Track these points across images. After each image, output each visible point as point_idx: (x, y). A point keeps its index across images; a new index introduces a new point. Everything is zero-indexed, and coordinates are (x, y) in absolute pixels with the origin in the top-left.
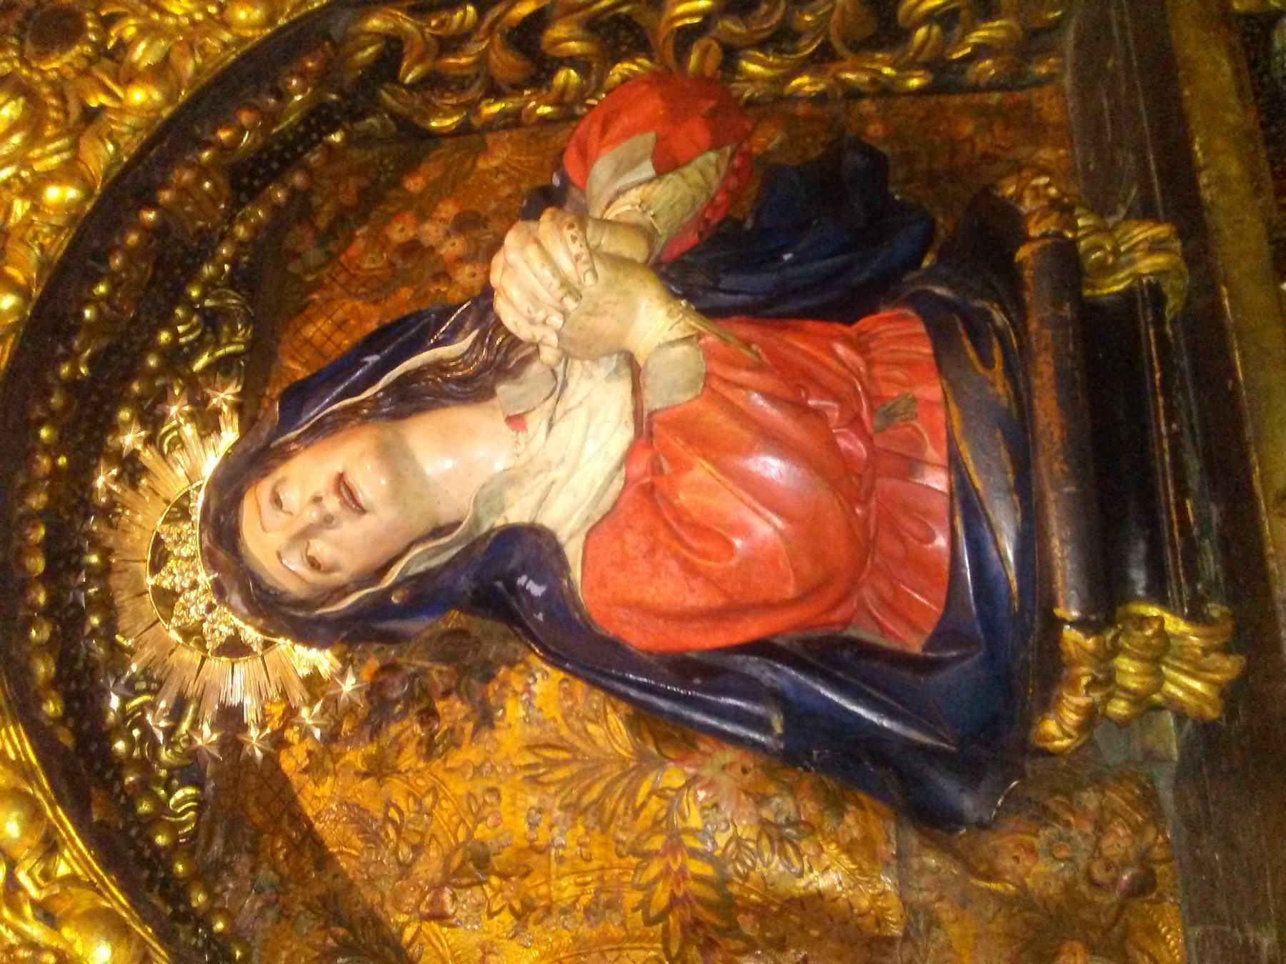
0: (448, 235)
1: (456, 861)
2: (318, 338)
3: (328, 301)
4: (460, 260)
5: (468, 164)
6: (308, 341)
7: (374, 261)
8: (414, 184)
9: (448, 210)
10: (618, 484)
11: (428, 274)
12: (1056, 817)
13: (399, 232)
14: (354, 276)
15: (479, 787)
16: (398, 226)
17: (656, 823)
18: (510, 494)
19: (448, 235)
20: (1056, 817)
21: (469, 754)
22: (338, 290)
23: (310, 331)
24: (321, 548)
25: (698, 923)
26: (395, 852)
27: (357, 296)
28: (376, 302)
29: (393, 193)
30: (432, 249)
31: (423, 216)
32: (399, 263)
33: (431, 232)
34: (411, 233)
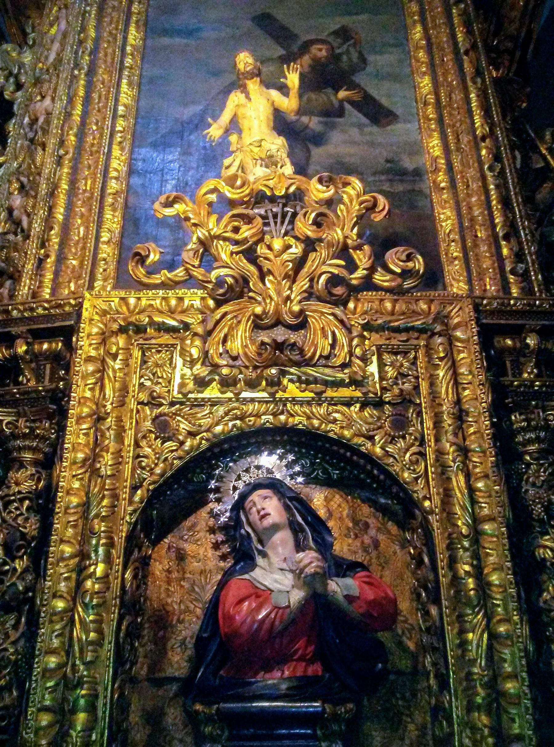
0: (371, 538)
1: (182, 552)
2: (335, 500)
3: (347, 502)
4: (363, 542)
5: (397, 543)
6: (334, 496)
7: (362, 514)
8: (391, 525)
9: (381, 537)
10: (263, 588)
11: (357, 532)
12: (184, 728)
13: (372, 521)
14: (356, 509)
15: (201, 556)
16: (374, 521)
17: (188, 607)
18: (266, 560)
19: (371, 538)
20: (184, 728)
21: (210, 553)
22: (351, 504)
23: (337, 496)
24: (254, 509)
25: (162, 619)
26: (186, 535)
27: (349, 510)
28: (348, 516)
29: (386, 519)
30: (366, 533)
31: (379, 530)
32: (362, 522)
33: (372, 532)
34: (372, 526)
